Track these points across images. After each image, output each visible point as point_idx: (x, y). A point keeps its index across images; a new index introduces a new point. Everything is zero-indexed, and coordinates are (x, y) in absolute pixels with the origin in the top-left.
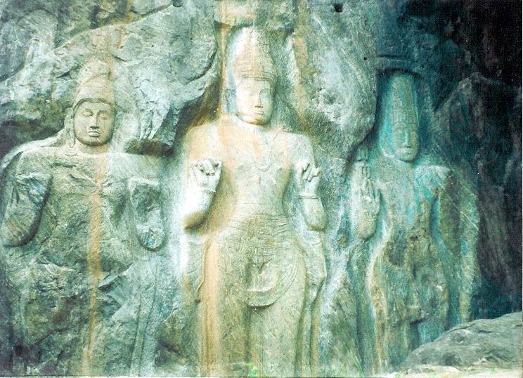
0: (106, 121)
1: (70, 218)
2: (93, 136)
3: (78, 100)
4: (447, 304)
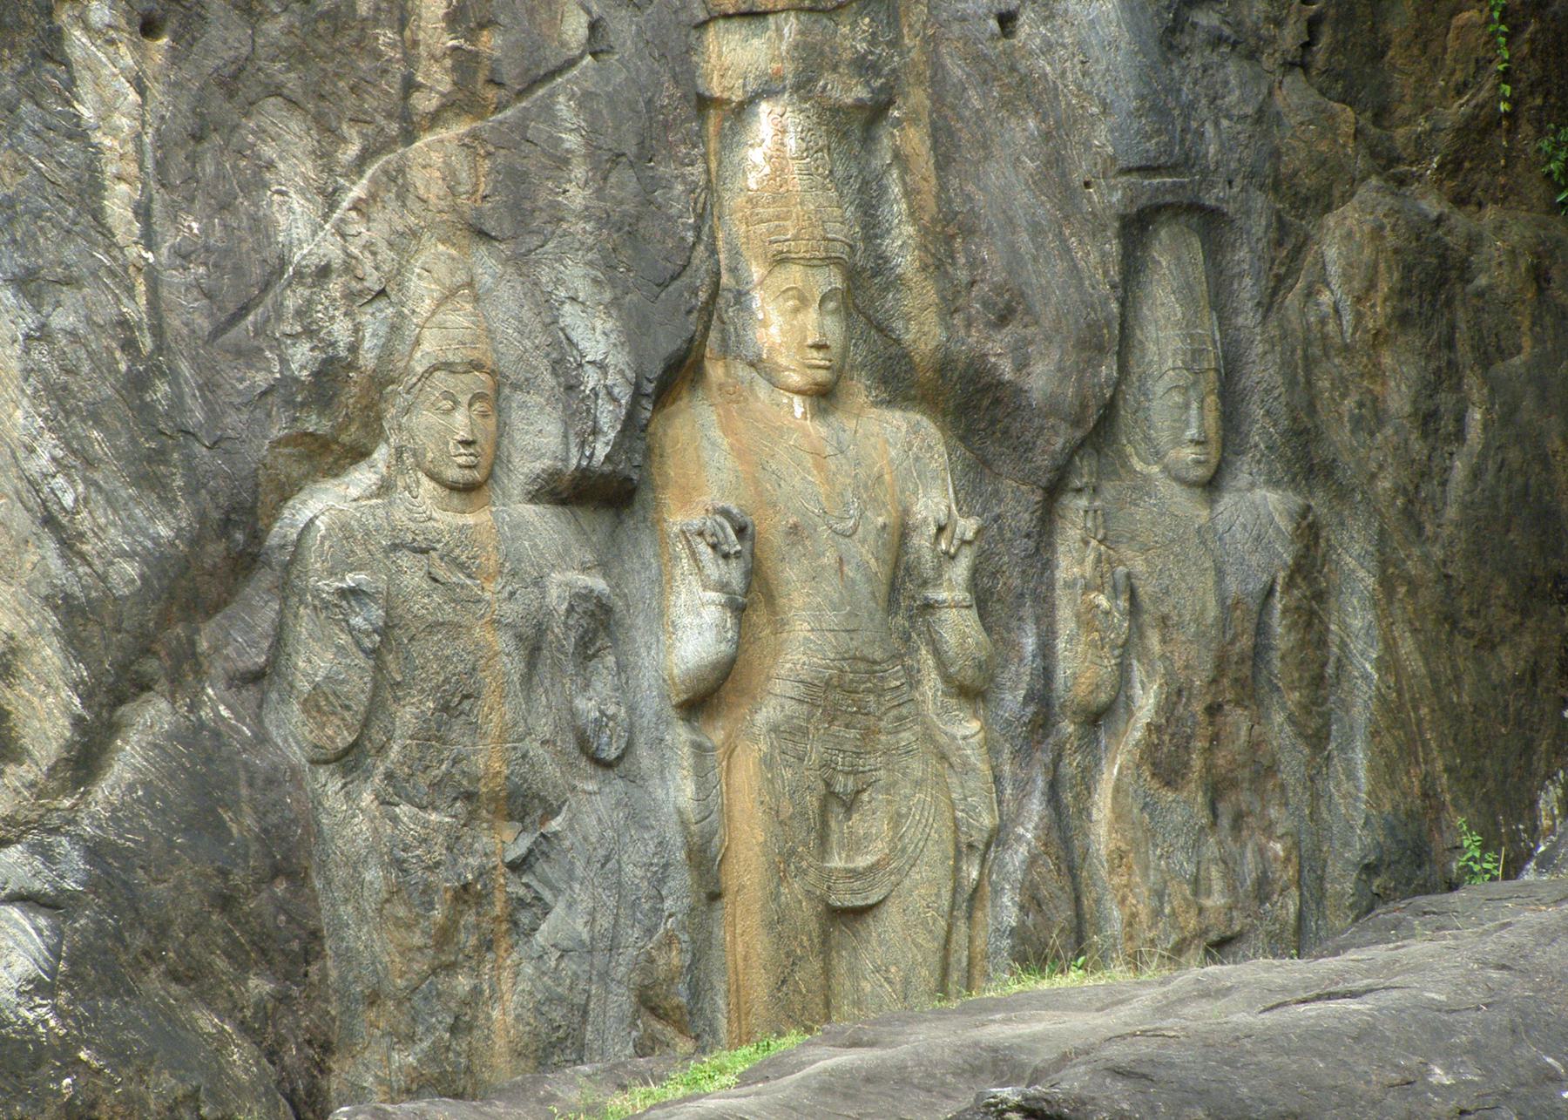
2: (469, 467)
3: (420, 370)
4: (1294, 891)
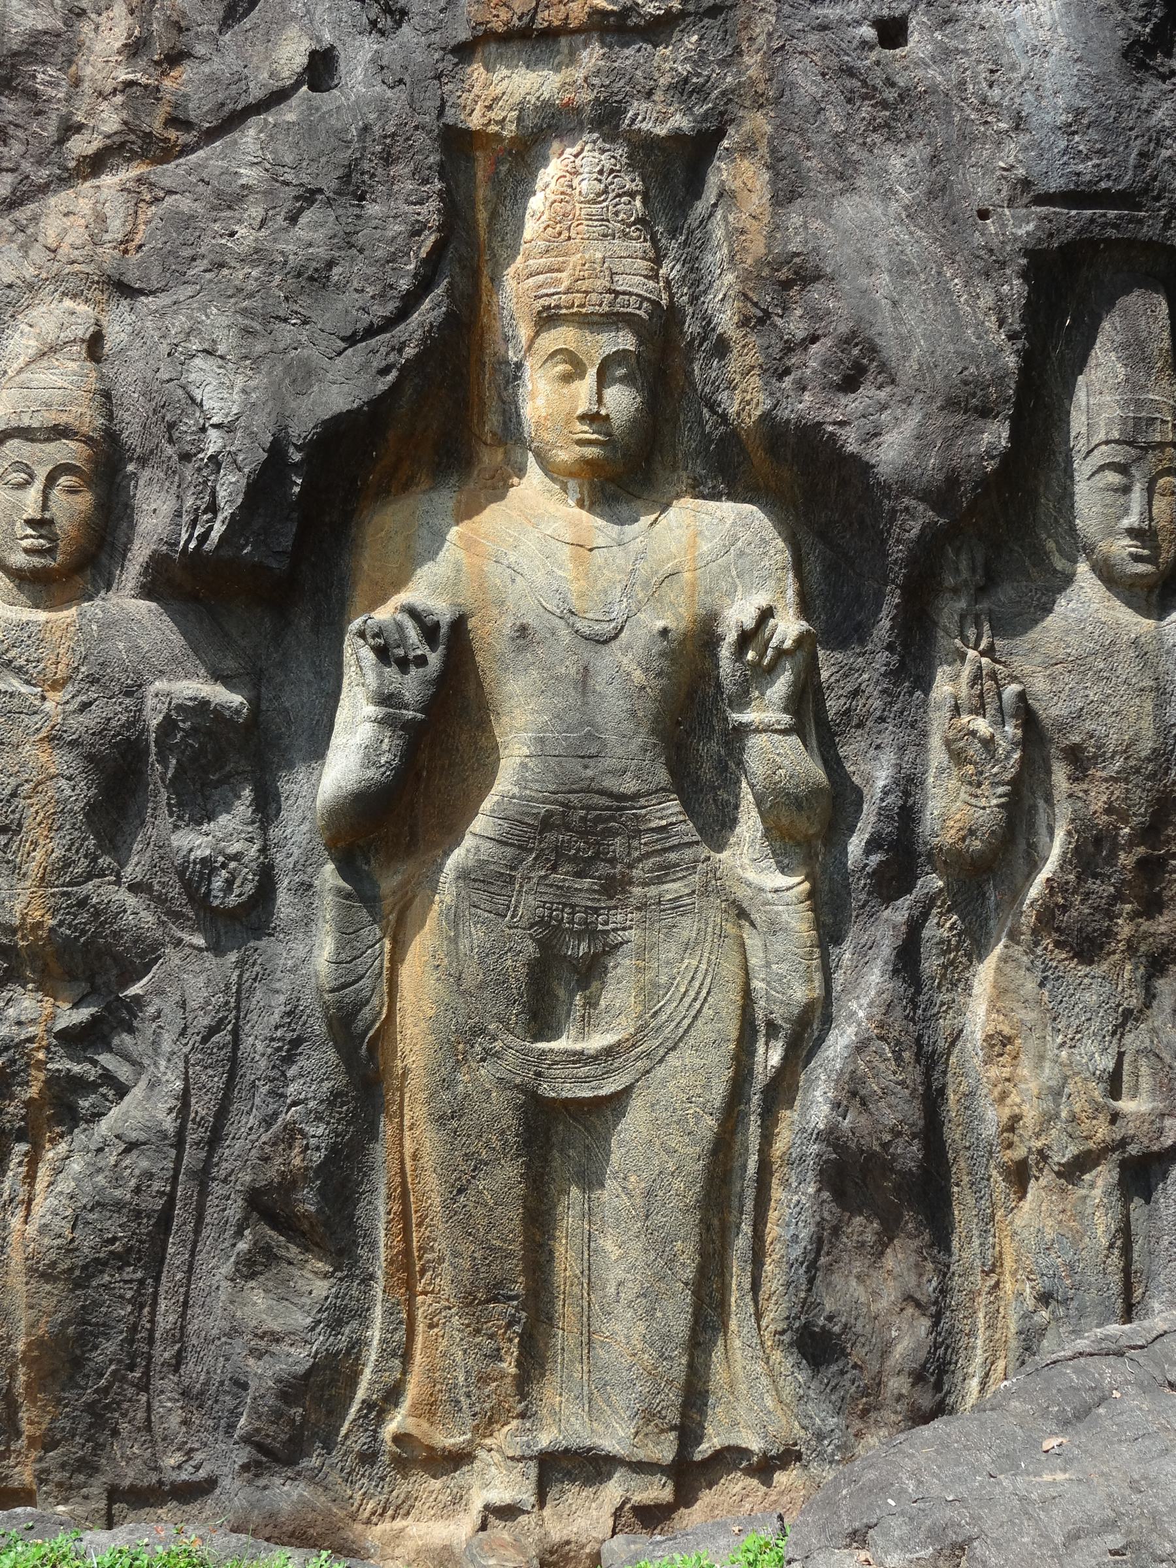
0: (78, 498)
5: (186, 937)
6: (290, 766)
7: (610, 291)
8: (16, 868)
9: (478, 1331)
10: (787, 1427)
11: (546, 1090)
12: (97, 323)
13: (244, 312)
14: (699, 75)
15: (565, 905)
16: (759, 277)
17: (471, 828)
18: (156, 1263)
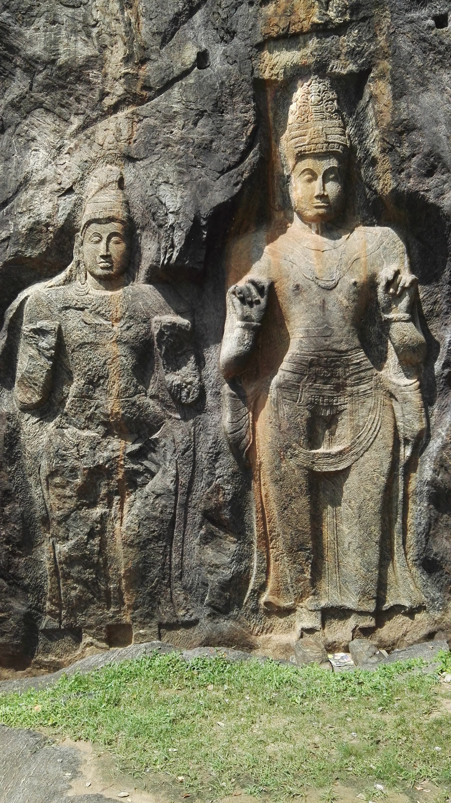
0: (120, 246)
1: (85, 373)
3: (83, 223)
5: (173, 415)
6: (208, 346)
7: (326, 142)
8: (107, 392)
9: (295, 562)
10: (419, 597)
11: (316, 468)
12: (121, 174)
13: (179, 164)
14: (359, 47)
15: (320, 396)
16: (389, 131)
17: (281, 367)
18: (170, 539)
